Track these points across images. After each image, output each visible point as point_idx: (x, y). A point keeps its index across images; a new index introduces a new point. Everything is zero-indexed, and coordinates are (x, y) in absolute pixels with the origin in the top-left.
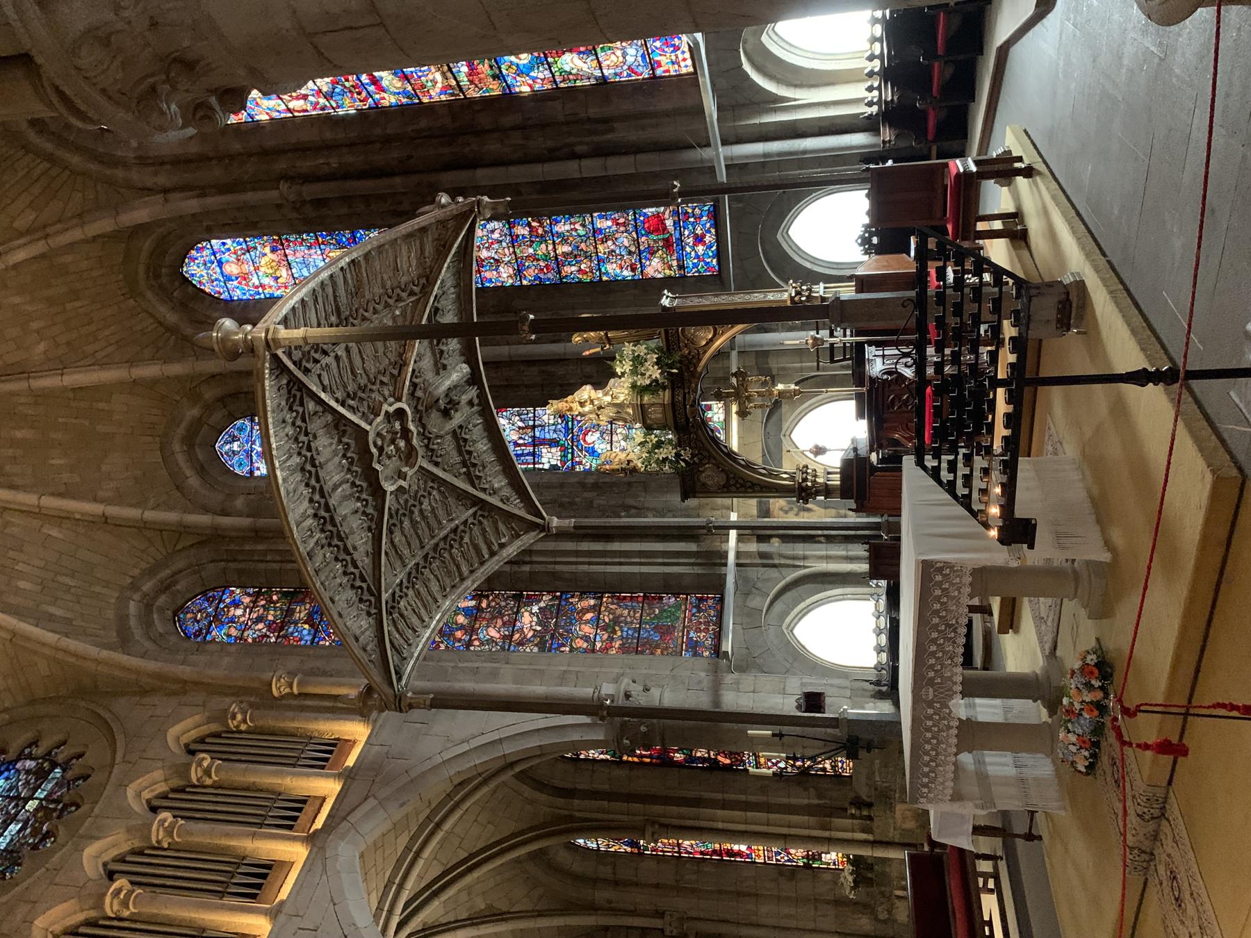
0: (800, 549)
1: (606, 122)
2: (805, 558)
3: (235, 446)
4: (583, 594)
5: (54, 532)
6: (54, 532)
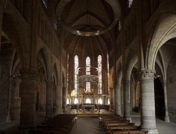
1: (96, 89)
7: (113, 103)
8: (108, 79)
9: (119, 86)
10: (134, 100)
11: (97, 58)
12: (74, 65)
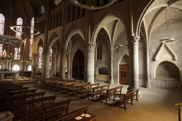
7: (36, 69)
8: (29, 45)
10: (55, 67)
11: (17, 20)
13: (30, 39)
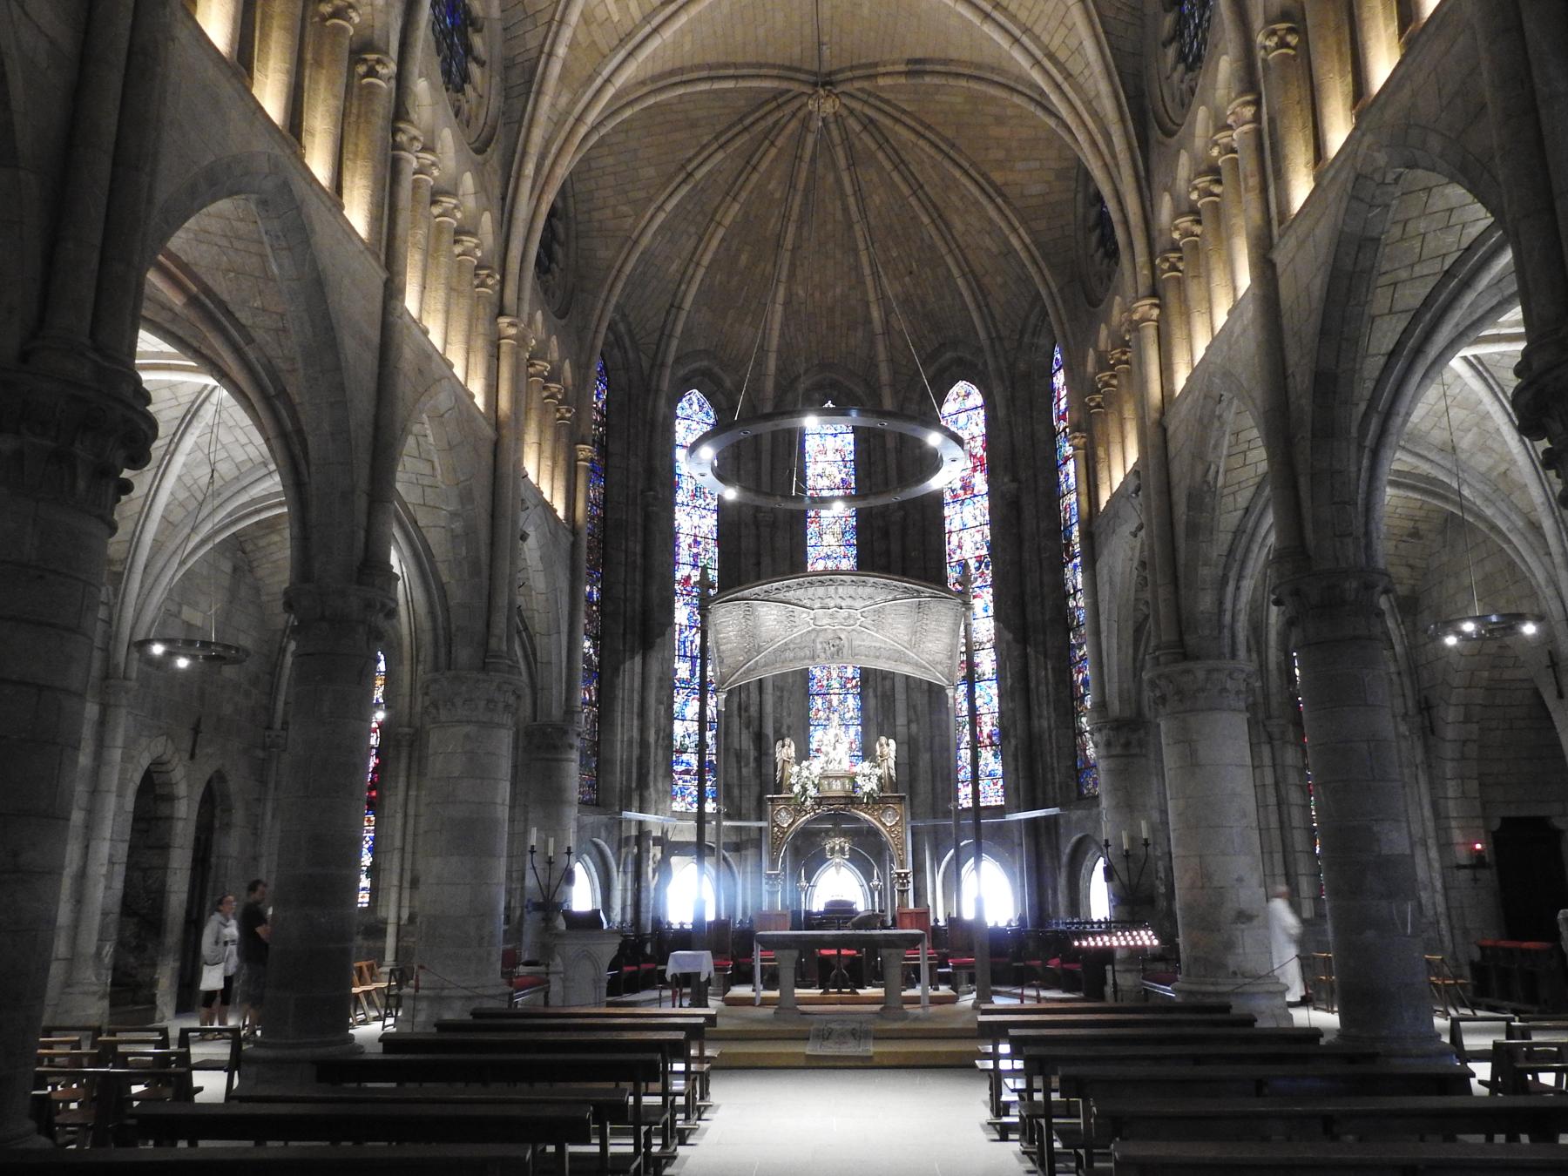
0: (630, 868)
2: (625, 872)
3: (696, 407)
4: (598, 691)
5: (674, 267)
6: (674, 267)
9: (1229, 684)
12: (673, 487)
13: (1064, 565)
